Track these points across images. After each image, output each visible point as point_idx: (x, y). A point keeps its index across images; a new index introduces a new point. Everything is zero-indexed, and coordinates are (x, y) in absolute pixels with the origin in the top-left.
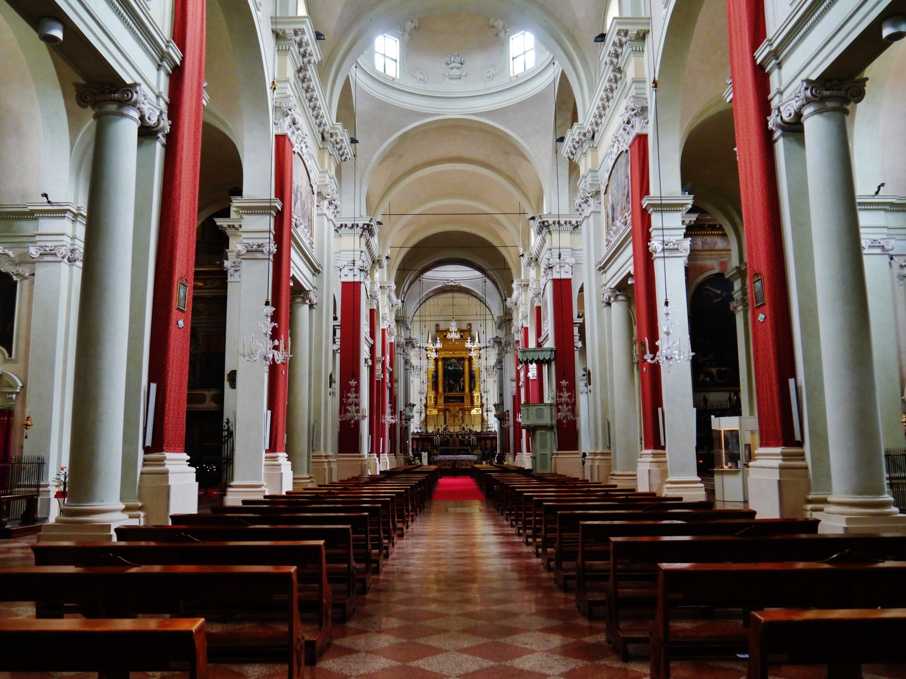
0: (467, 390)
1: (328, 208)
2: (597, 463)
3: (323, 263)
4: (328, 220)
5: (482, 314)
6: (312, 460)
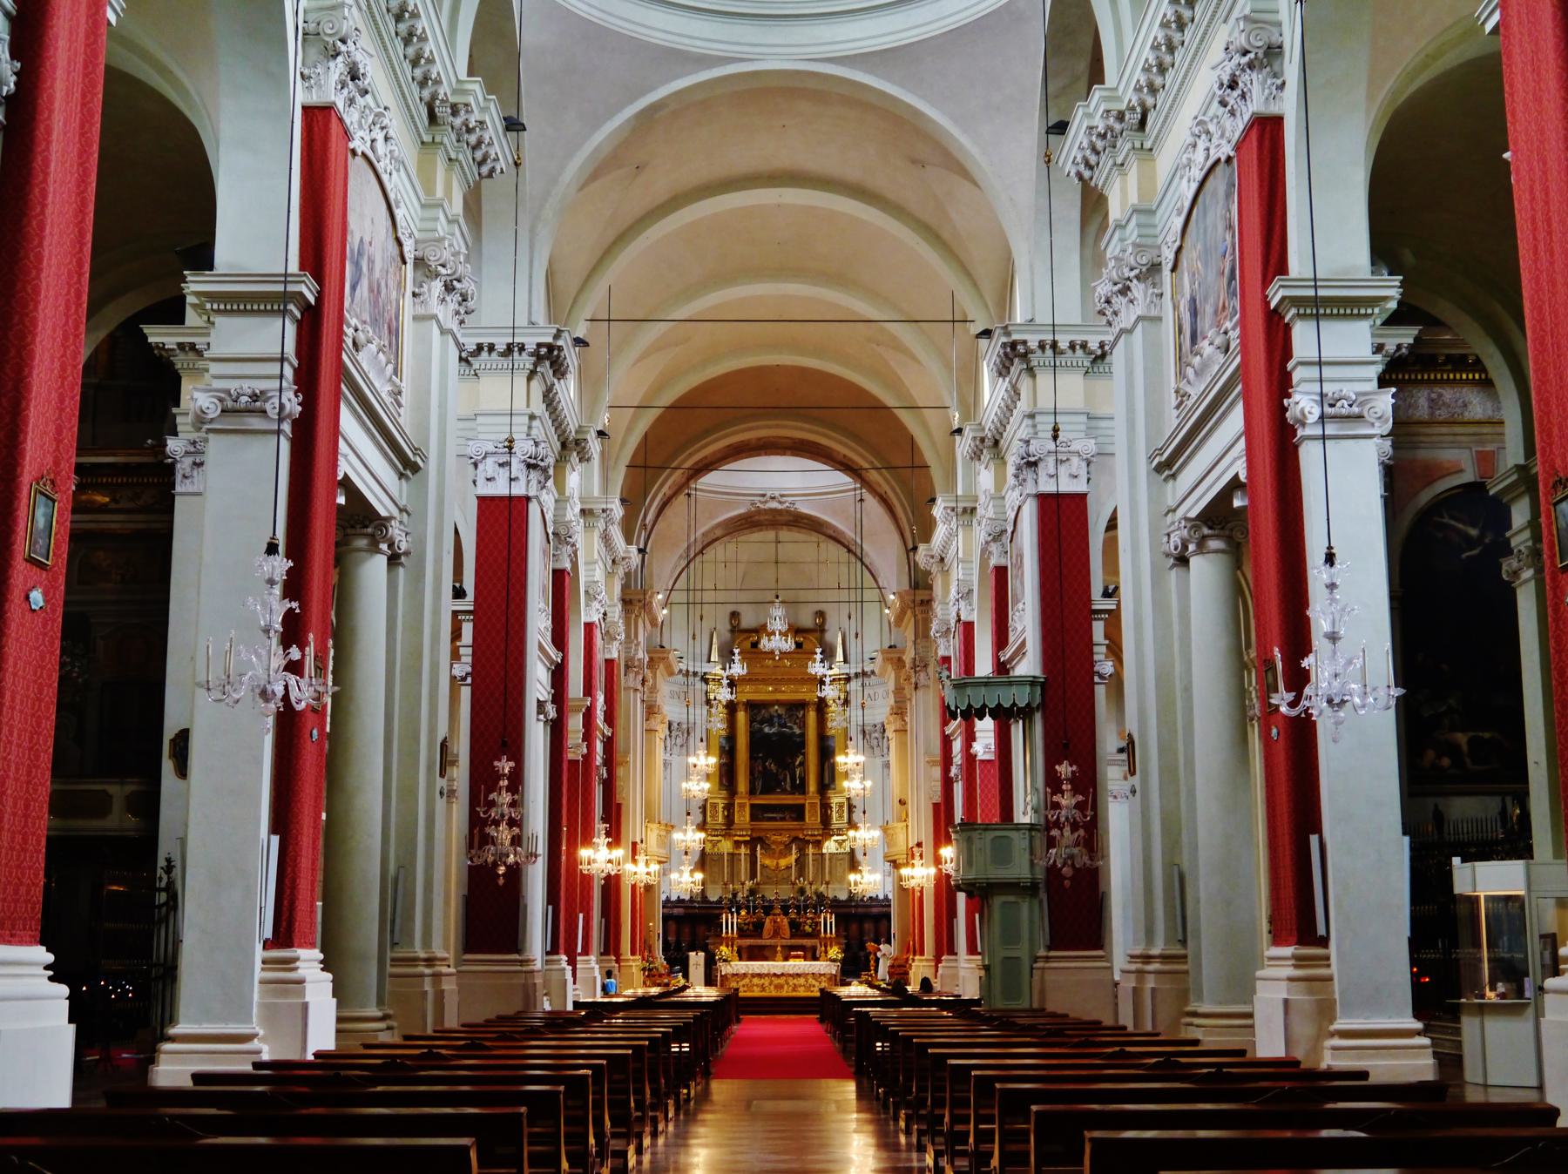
0: (812, 786)
1: (443, 300)
2: (1150, 982)
3: (427, 442)
4: (443, 332)
5: (853, 585)
6: (390, 970)
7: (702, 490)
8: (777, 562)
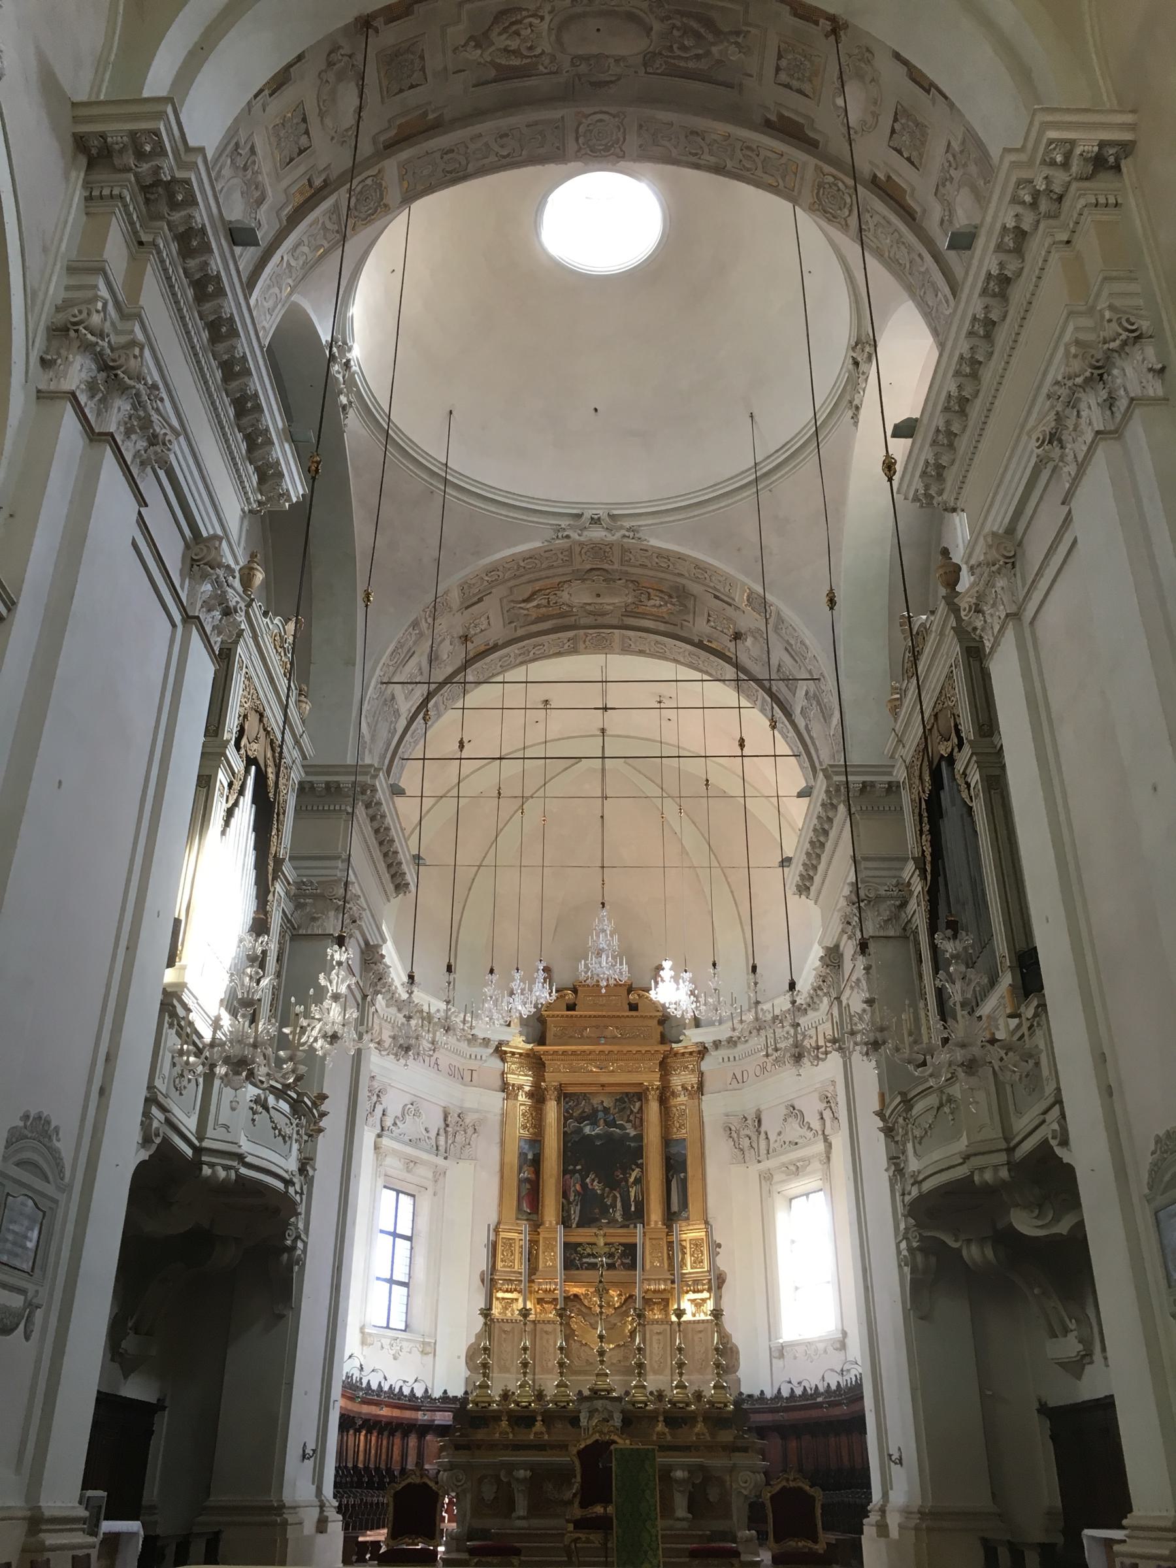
0: (655, 1215)
7: (451, 469)
8: (603, 867)
